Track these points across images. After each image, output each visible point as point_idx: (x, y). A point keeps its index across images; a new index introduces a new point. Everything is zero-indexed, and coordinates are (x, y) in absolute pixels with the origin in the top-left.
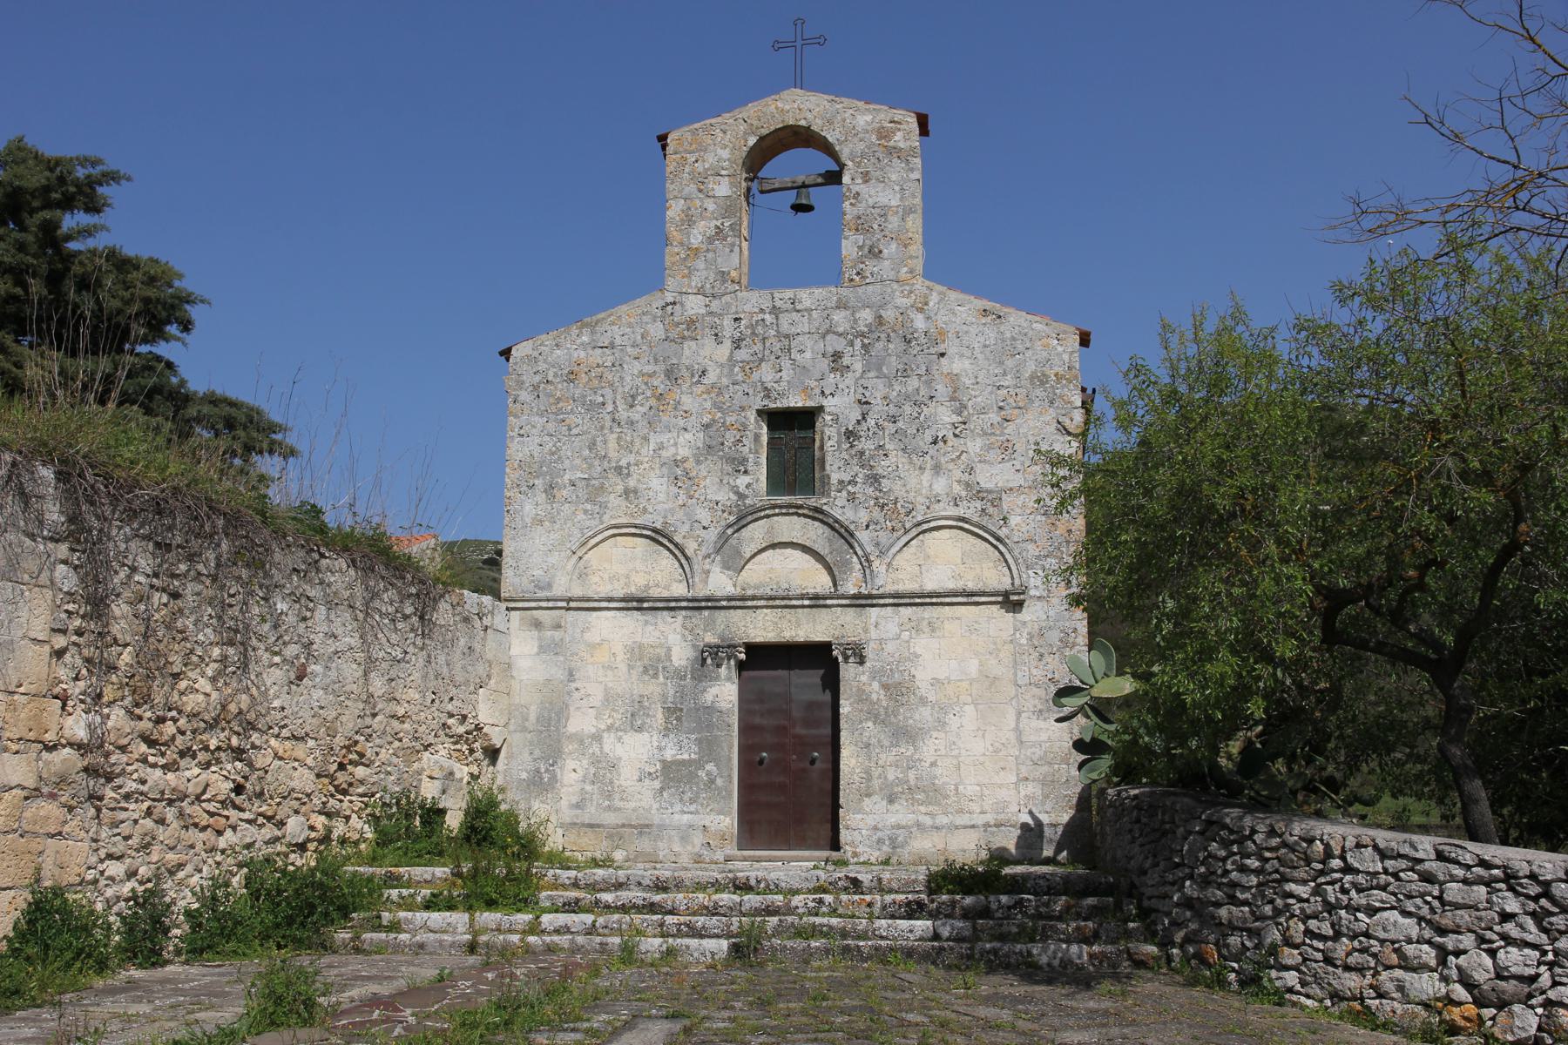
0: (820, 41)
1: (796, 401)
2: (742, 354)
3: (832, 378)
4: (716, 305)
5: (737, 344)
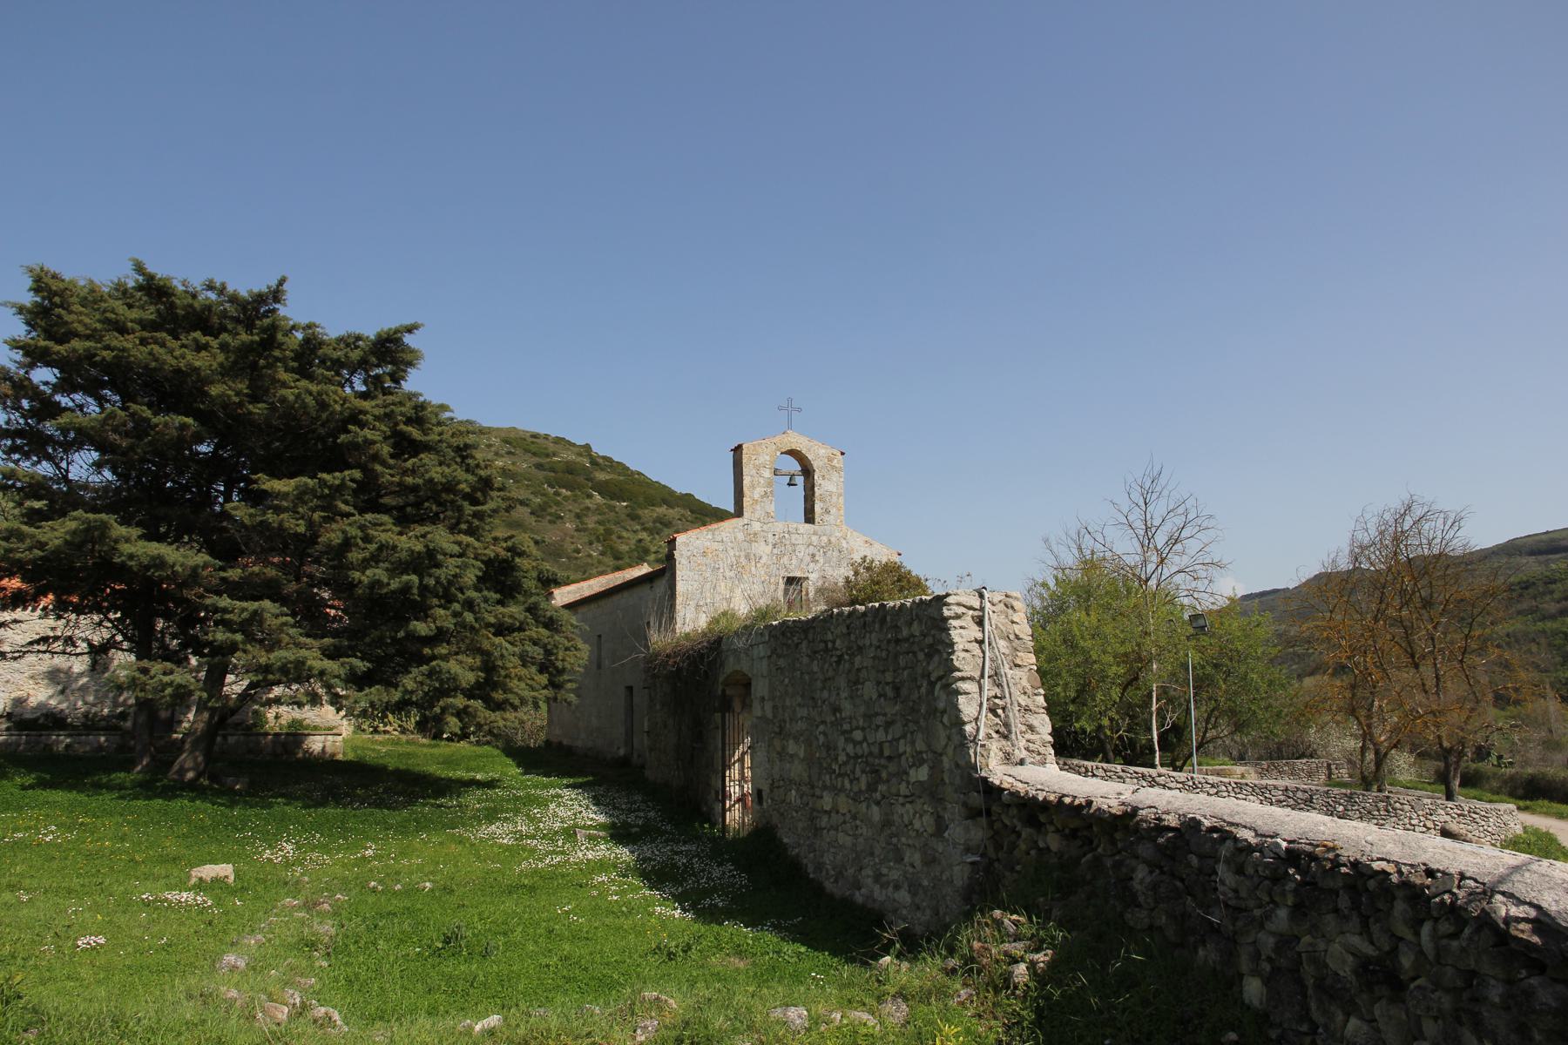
0: (799, 410)
1: (798, 574)
2: (775, 551)
3: (812, 565)
4: (765, 527)
5: (774, 546)
